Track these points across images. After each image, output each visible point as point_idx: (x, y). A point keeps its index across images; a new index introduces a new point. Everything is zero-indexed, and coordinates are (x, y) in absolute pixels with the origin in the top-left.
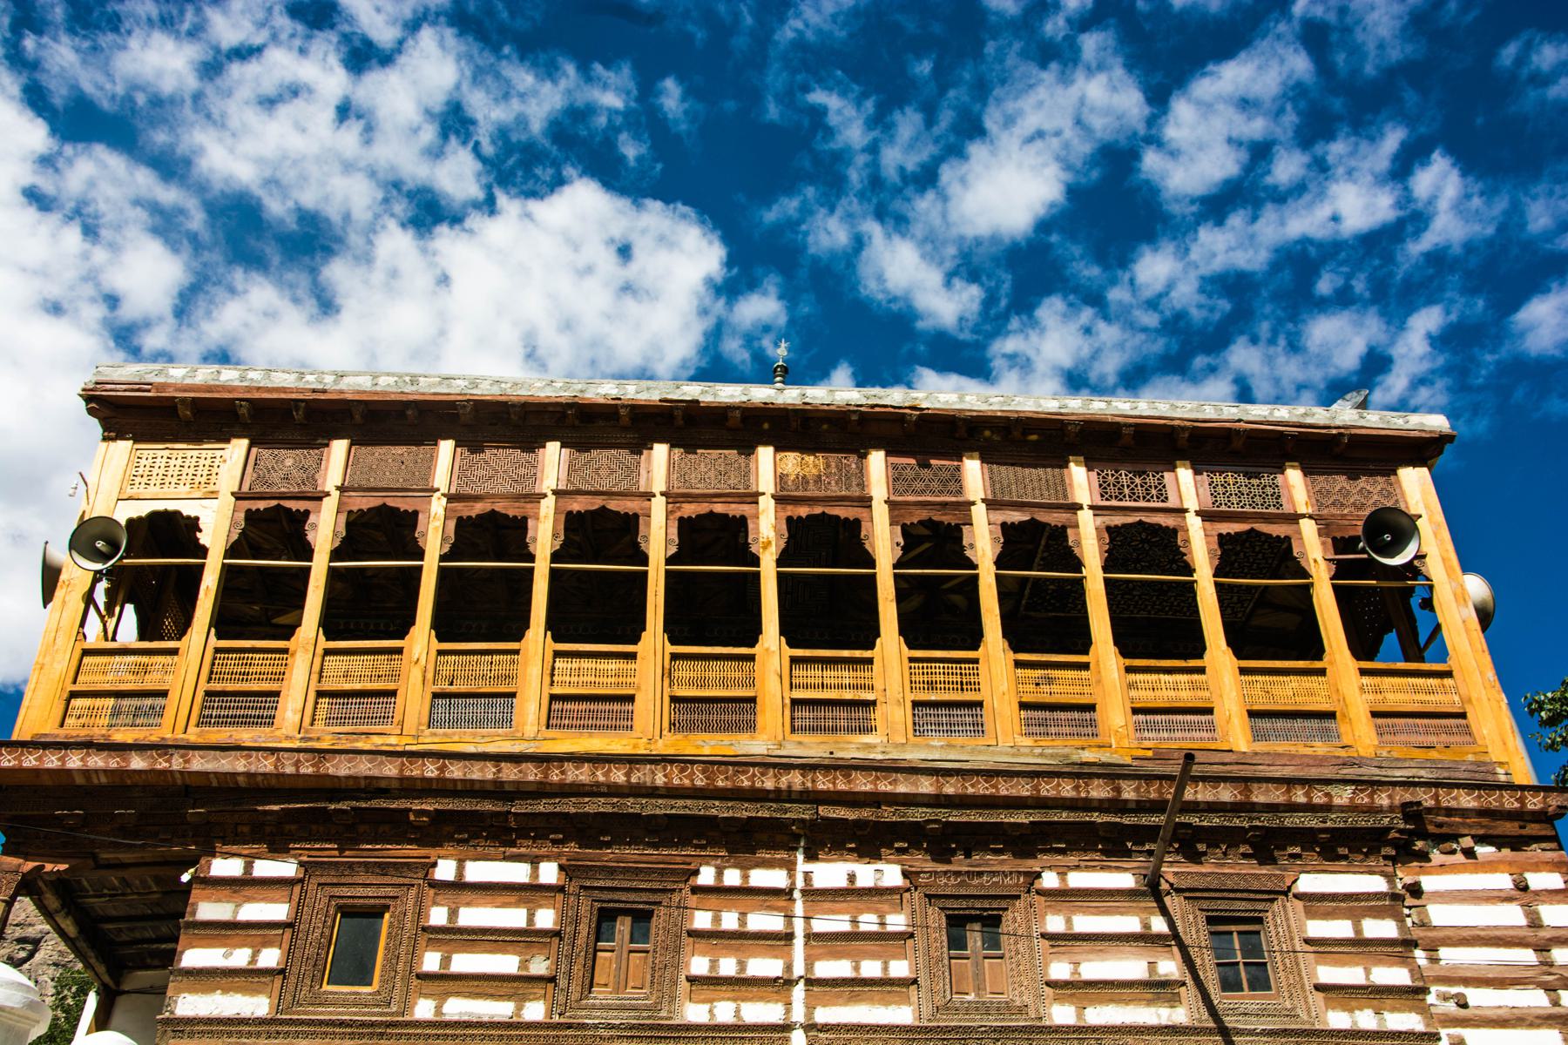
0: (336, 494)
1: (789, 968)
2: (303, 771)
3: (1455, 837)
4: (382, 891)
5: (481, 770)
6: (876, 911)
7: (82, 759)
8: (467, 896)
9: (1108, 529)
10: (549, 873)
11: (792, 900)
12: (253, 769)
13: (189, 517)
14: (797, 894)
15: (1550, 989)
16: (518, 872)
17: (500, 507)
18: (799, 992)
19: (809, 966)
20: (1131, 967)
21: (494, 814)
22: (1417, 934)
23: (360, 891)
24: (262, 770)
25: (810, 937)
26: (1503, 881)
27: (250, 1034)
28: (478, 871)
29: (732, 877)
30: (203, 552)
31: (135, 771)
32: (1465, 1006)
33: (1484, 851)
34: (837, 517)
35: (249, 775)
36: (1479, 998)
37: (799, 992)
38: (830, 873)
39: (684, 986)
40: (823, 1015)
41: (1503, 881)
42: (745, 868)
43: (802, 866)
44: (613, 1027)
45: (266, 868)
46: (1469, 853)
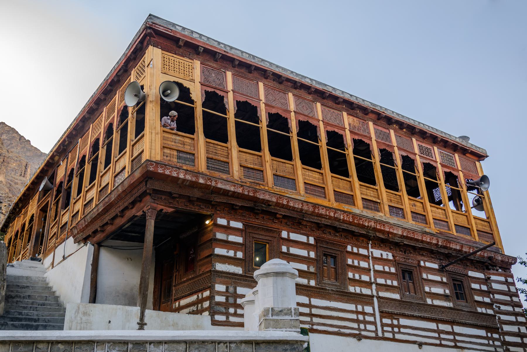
0: (232, 92)
1: (370, 279)
2: (250, 194)
3: (496, 266)
4: (267, 238)
5: (298, 205)
6: (388, 266)
7: (184, 175)
8: (291, 244)
9: (424, 163)
10: (312, 240)
11: (369, 259)
12: (236, 190)
13: (186, 87)
14: (370, 258)
15: (513, 307)
16: (303, 238)
17: (280, 112)
18: (374, 286)
19: (375, 279)
20: (439, 290)
21: (298, 220)
22: (491, 290)
23: (261, 237)
24: (238, 191)
25: (375, 271)
26: (502, 279)
27: (238, 279)
28: (294, 236)
29: (355, 250)
30: (192, 102)
31: (200, 183)
32: (499, 309)
33: (500, 270)
34: (364, 142)
35: (234, 192)
36: (503, 308)
37: (374, 286)
38: (377, 253)
39: (348, 280)
40: (381, 294)
41: (502, 279)
42: (358, 247)
43: (371, 250)
44: (333, 290)
45: (234, 224)
46: (497, 270)
